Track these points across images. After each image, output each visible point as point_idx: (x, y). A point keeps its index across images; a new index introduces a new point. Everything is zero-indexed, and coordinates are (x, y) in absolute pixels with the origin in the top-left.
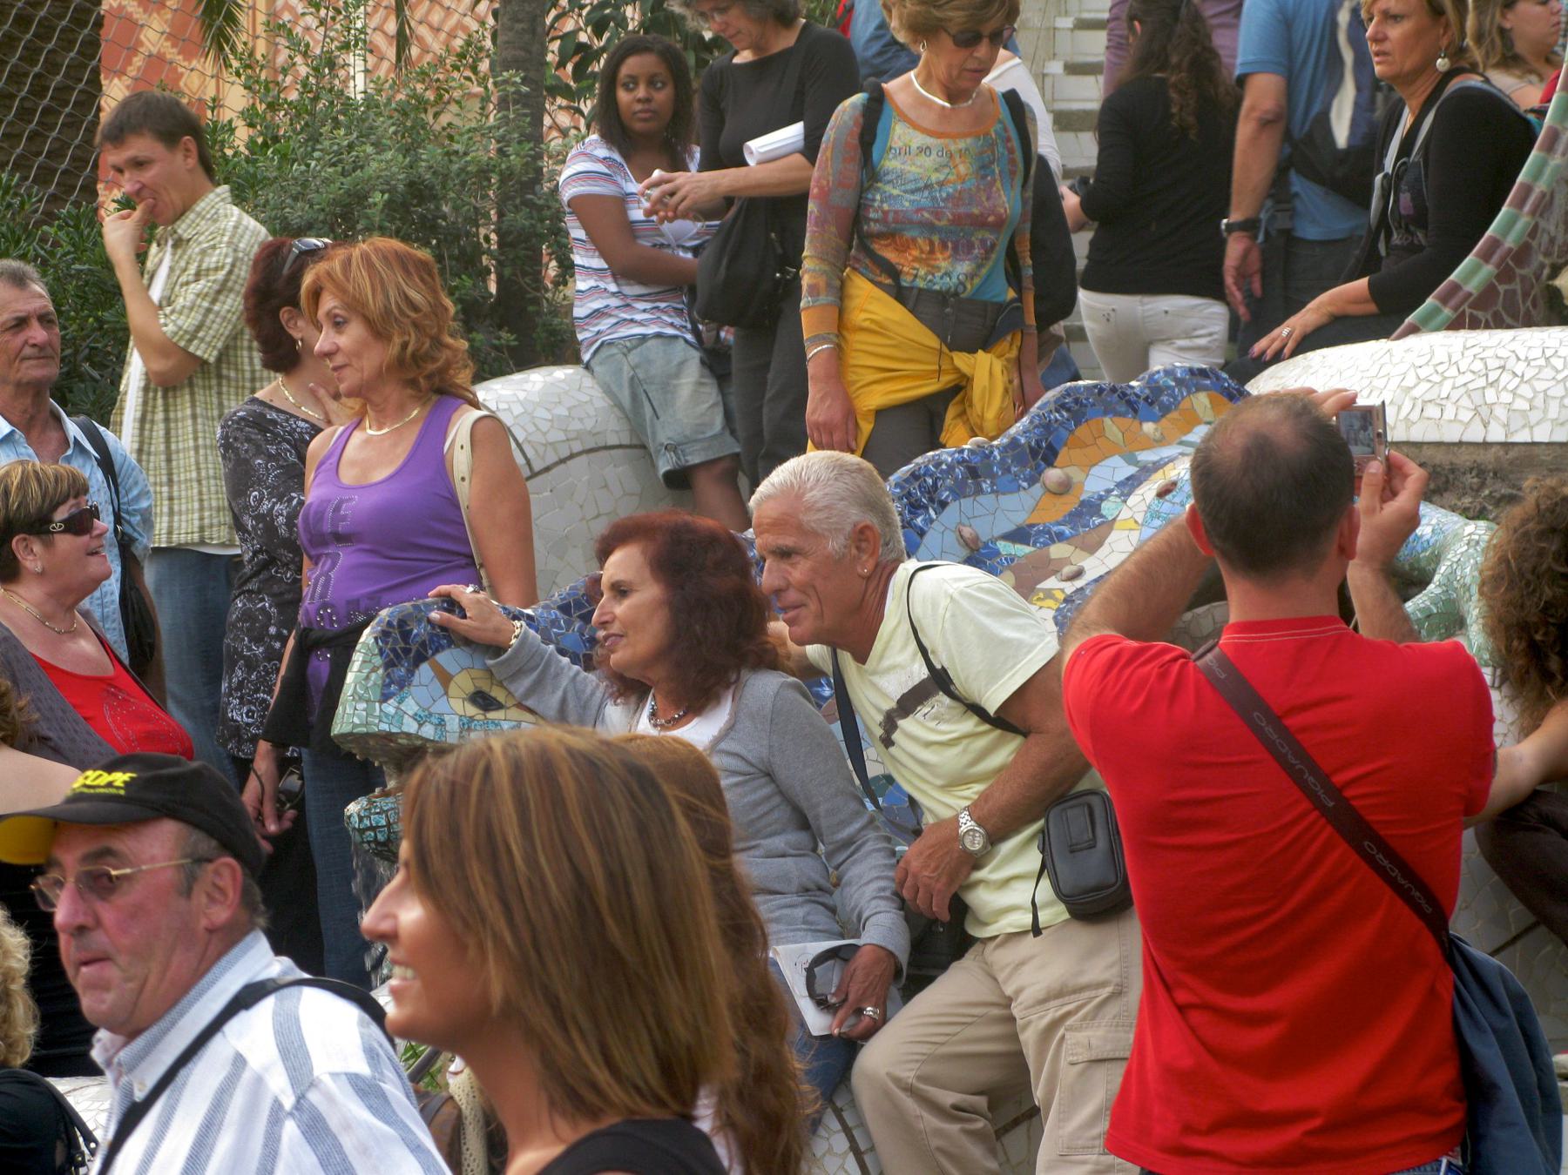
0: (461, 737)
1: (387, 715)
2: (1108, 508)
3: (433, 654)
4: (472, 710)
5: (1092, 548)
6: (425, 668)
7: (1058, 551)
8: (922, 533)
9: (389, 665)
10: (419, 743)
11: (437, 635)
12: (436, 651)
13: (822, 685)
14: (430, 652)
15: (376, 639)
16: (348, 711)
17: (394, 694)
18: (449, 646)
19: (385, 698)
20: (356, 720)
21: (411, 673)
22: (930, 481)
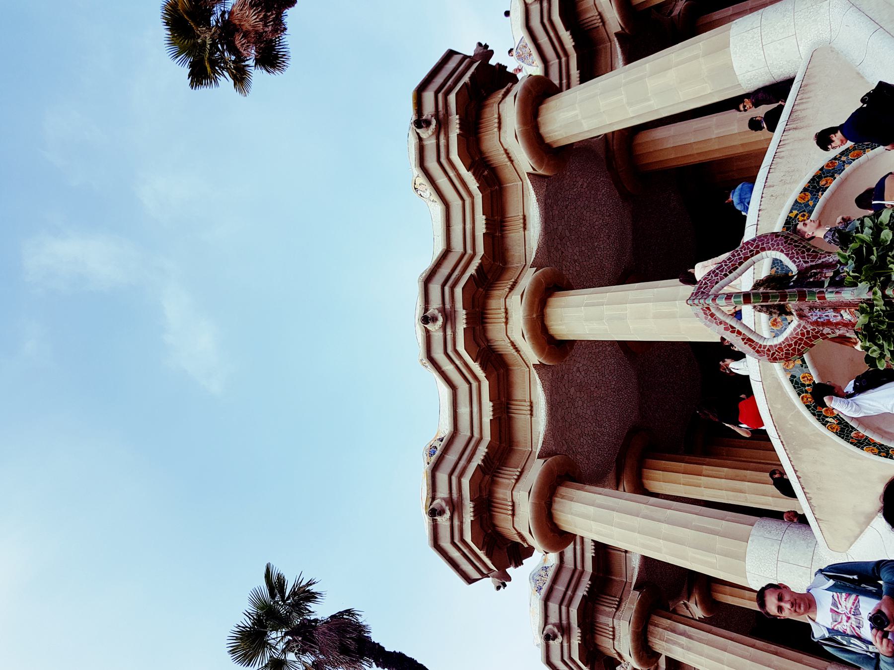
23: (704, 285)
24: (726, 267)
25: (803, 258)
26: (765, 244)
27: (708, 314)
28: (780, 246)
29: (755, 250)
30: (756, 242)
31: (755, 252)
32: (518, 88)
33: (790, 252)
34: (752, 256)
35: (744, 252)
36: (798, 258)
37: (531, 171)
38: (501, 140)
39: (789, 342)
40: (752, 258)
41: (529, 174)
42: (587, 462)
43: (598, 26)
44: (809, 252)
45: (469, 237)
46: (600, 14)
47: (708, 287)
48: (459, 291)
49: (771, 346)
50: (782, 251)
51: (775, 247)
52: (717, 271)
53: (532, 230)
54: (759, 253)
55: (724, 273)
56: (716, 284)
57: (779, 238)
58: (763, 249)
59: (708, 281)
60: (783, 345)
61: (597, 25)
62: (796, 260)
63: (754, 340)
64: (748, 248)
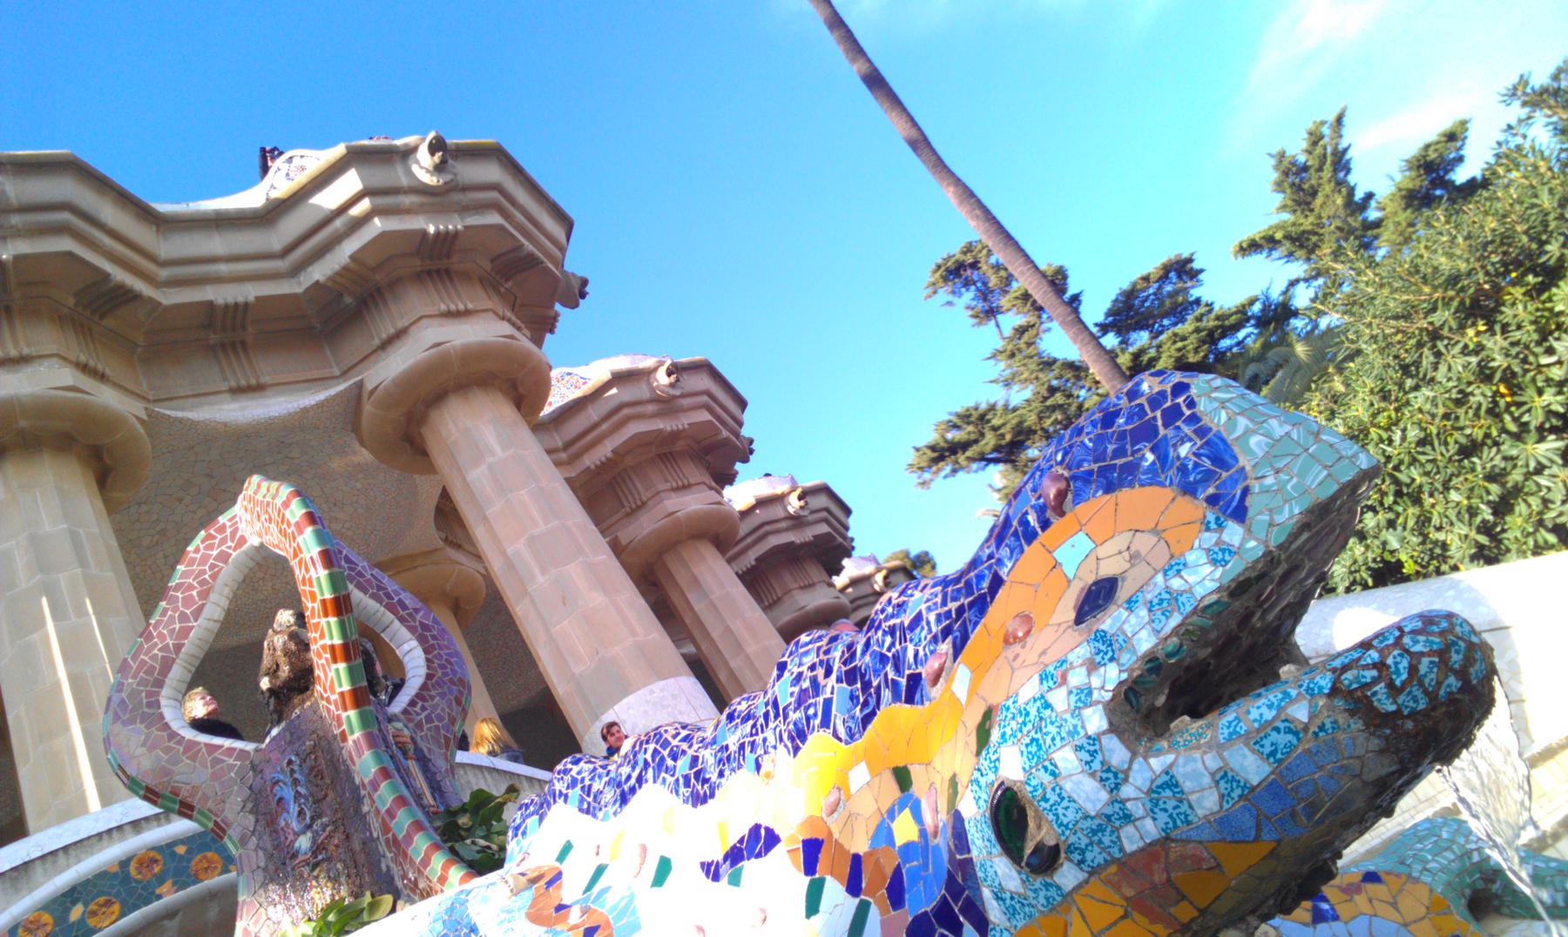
27: (223, 548)
32: (525, 342)
34: (402, 620)
36: (424, 709)
37: (369, 386)
38: (424, 322)
40: (397, 623)
41: (360, 385)
43: (623, 507)
45: (194, 271)
46: (644, 504)
48: (65, 244)
49: (161, 717)
50: (429, 677)
53: (233, 406)
60: (172, 744)
61: (626, 504)
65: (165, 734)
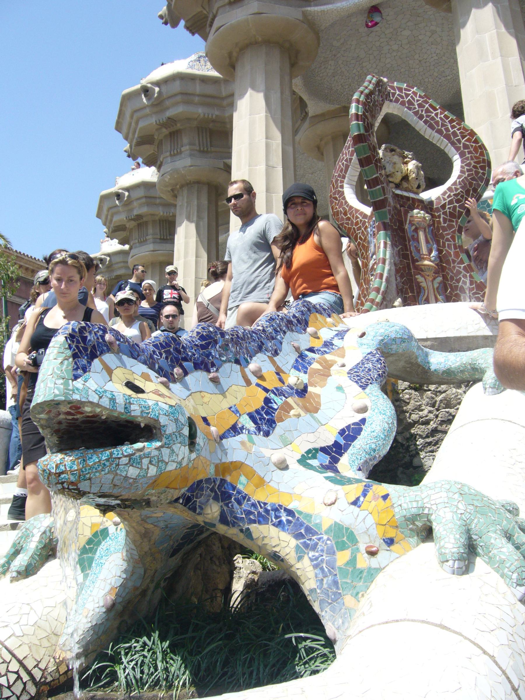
0: (126, 408)
1: (77, 389)
2: (336, 342)
3: (100, 355)
4: (129, 392)
5: (343, 356)
6: (96, 361)
7: (328, 357)
8: (281, 343)
9: (75, 356)
10: (98, 410)
11: (100, 343)
12: (102, 353)
13: (272, 403)
14: (98, 353)
15: (66, 337)
16: (49, 385)
17: (81, 376)
18: (108, 352)
19: (76, 377)
20: (57, 392)
21: (90, 363)
22: (278, 322)
23: (405, 94)
24: (433, 115)
25: (450, 202)
26: (469, 155)
28: (467, 173)
29: (462, 145)
30: (474, 144)
31: (459, 145)
33: (458, 187)
34: (453, 144)
35: (458, 132)
36: (449, 196)
39: (349, 211)
42: (329, 74)
44: (459, 208)
47: (401, 100)
50: (459, 177)
51: (466, 167)
52: (427, 106)
54: (457, 151)
55: (425, 115)
56: (408, 108)
57: (480, 170)
58: (462, 155)
59: (412, 97)
62: (447, 195)
63: (348, 173)
64: (463, 137)
65: (344, 201)
